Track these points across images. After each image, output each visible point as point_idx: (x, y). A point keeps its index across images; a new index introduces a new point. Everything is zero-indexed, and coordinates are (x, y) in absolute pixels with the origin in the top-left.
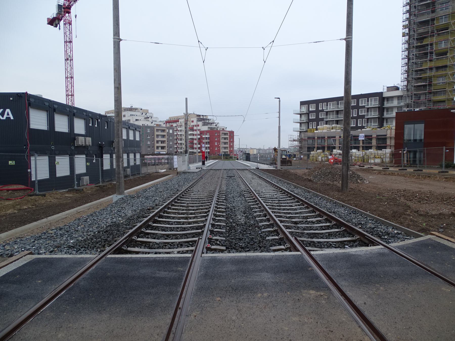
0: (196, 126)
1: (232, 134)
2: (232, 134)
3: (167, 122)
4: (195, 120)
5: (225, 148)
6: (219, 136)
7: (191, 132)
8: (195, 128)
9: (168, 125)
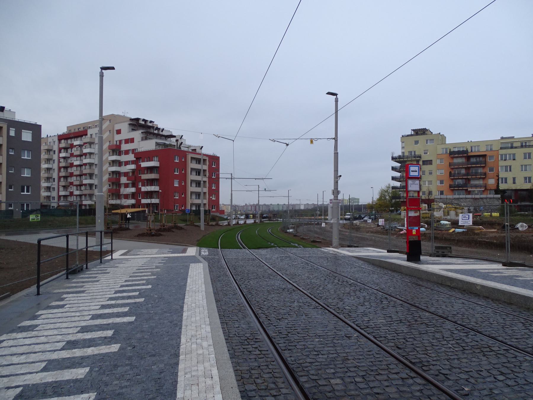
0: (127, 141)
1: (214, 160)
2: (214, 160)
3: (61, 138)
4: (125, 127)
5: (198, 195)
6: (183, 166)
7: (114, 158)
8: (125, 147)
9: (63, 144)
